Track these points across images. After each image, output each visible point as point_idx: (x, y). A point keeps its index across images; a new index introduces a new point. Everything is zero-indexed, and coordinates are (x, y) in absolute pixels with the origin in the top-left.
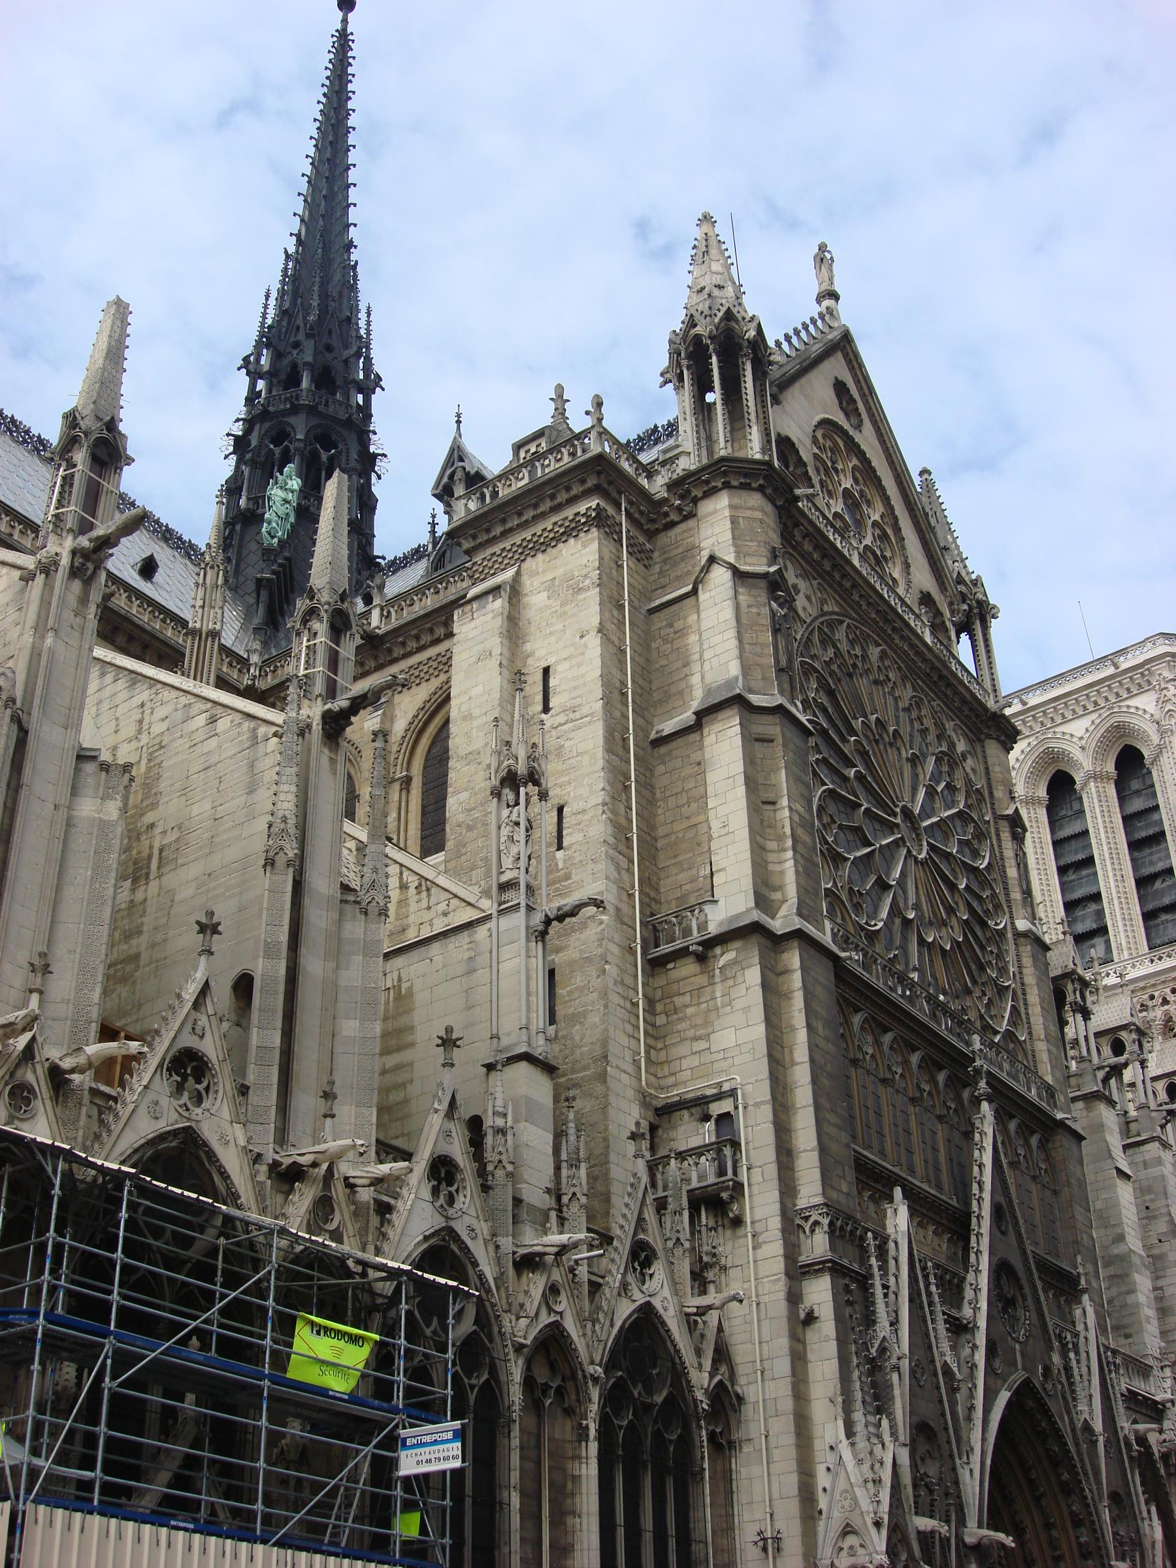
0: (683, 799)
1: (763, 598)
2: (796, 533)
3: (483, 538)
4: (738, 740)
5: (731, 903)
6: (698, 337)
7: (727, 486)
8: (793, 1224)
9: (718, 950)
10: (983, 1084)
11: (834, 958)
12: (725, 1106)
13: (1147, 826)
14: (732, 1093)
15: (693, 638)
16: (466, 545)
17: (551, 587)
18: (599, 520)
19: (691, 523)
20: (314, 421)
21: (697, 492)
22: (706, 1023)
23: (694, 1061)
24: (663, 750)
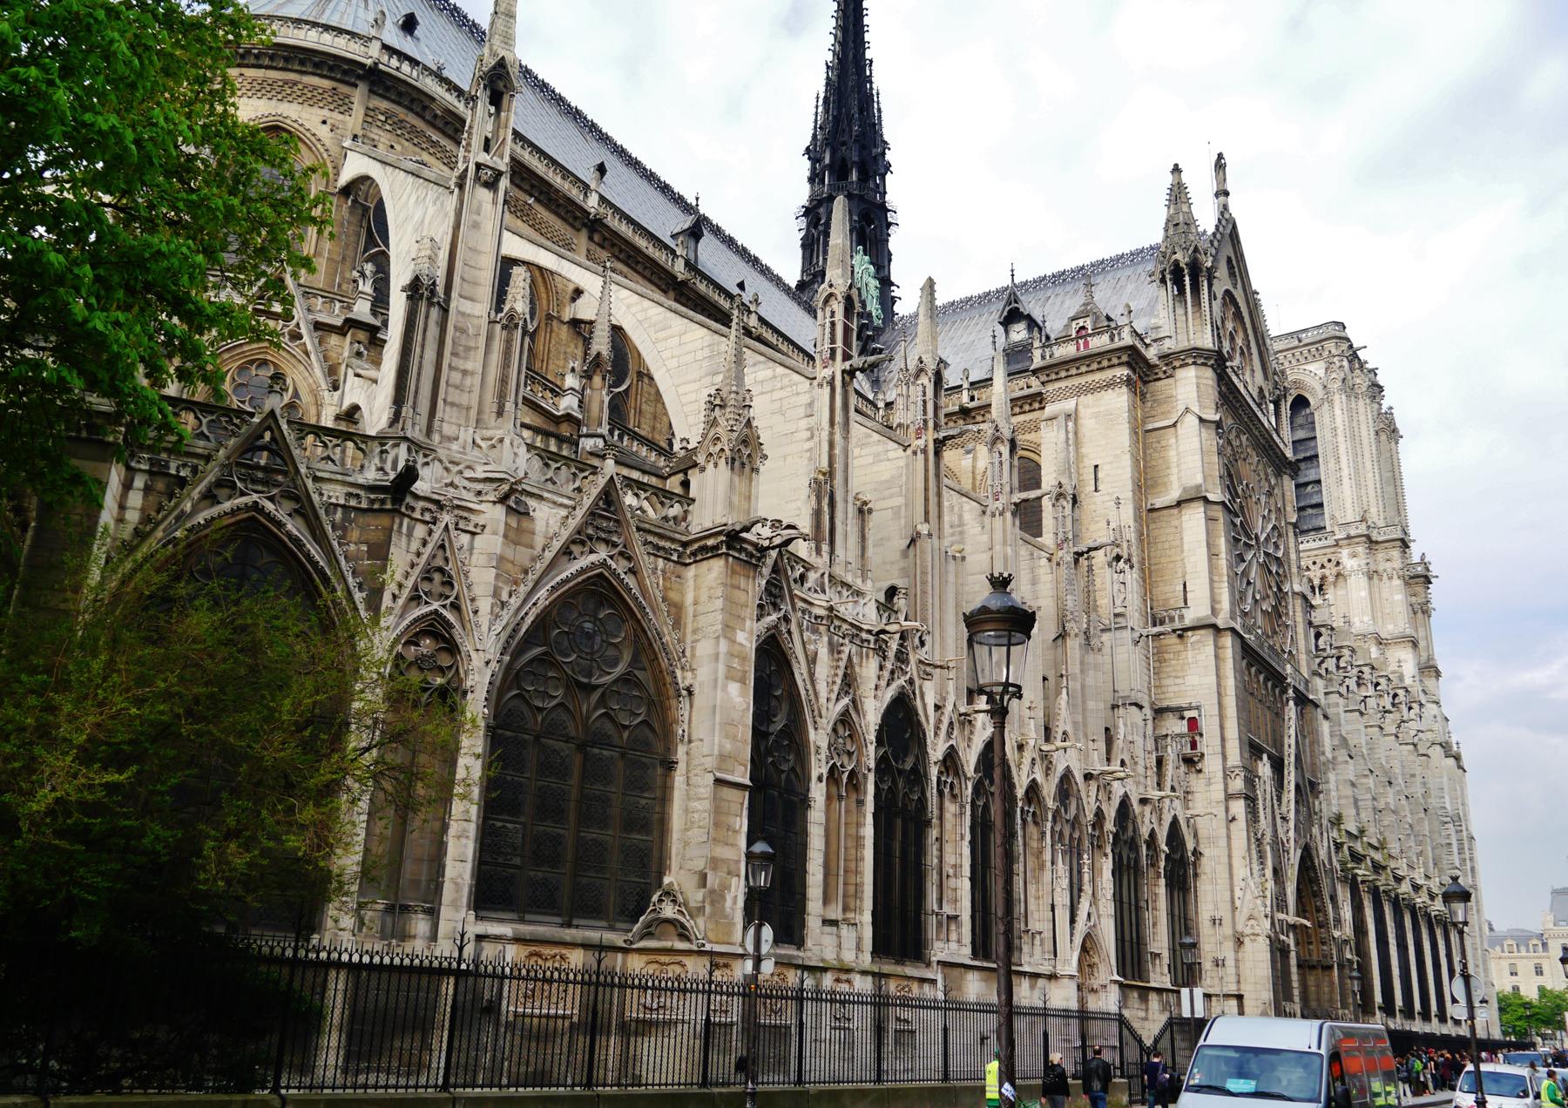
2: (1229, 396)
3: (1053, 377)
5: (1197, 610)
6: (1176, 261)
8: (1227, 775)
10: (1290, 691)
11: (1242, 637)
12: (1193, 714)
14: (1198, 708)
15: (1172, 453)
16: (1044, 378)
17: (1096, 416)
18: (1129, 382)
19: (1170, 380)
20: (863, 206)
21: (1177, 364)
24: (1155, 515)
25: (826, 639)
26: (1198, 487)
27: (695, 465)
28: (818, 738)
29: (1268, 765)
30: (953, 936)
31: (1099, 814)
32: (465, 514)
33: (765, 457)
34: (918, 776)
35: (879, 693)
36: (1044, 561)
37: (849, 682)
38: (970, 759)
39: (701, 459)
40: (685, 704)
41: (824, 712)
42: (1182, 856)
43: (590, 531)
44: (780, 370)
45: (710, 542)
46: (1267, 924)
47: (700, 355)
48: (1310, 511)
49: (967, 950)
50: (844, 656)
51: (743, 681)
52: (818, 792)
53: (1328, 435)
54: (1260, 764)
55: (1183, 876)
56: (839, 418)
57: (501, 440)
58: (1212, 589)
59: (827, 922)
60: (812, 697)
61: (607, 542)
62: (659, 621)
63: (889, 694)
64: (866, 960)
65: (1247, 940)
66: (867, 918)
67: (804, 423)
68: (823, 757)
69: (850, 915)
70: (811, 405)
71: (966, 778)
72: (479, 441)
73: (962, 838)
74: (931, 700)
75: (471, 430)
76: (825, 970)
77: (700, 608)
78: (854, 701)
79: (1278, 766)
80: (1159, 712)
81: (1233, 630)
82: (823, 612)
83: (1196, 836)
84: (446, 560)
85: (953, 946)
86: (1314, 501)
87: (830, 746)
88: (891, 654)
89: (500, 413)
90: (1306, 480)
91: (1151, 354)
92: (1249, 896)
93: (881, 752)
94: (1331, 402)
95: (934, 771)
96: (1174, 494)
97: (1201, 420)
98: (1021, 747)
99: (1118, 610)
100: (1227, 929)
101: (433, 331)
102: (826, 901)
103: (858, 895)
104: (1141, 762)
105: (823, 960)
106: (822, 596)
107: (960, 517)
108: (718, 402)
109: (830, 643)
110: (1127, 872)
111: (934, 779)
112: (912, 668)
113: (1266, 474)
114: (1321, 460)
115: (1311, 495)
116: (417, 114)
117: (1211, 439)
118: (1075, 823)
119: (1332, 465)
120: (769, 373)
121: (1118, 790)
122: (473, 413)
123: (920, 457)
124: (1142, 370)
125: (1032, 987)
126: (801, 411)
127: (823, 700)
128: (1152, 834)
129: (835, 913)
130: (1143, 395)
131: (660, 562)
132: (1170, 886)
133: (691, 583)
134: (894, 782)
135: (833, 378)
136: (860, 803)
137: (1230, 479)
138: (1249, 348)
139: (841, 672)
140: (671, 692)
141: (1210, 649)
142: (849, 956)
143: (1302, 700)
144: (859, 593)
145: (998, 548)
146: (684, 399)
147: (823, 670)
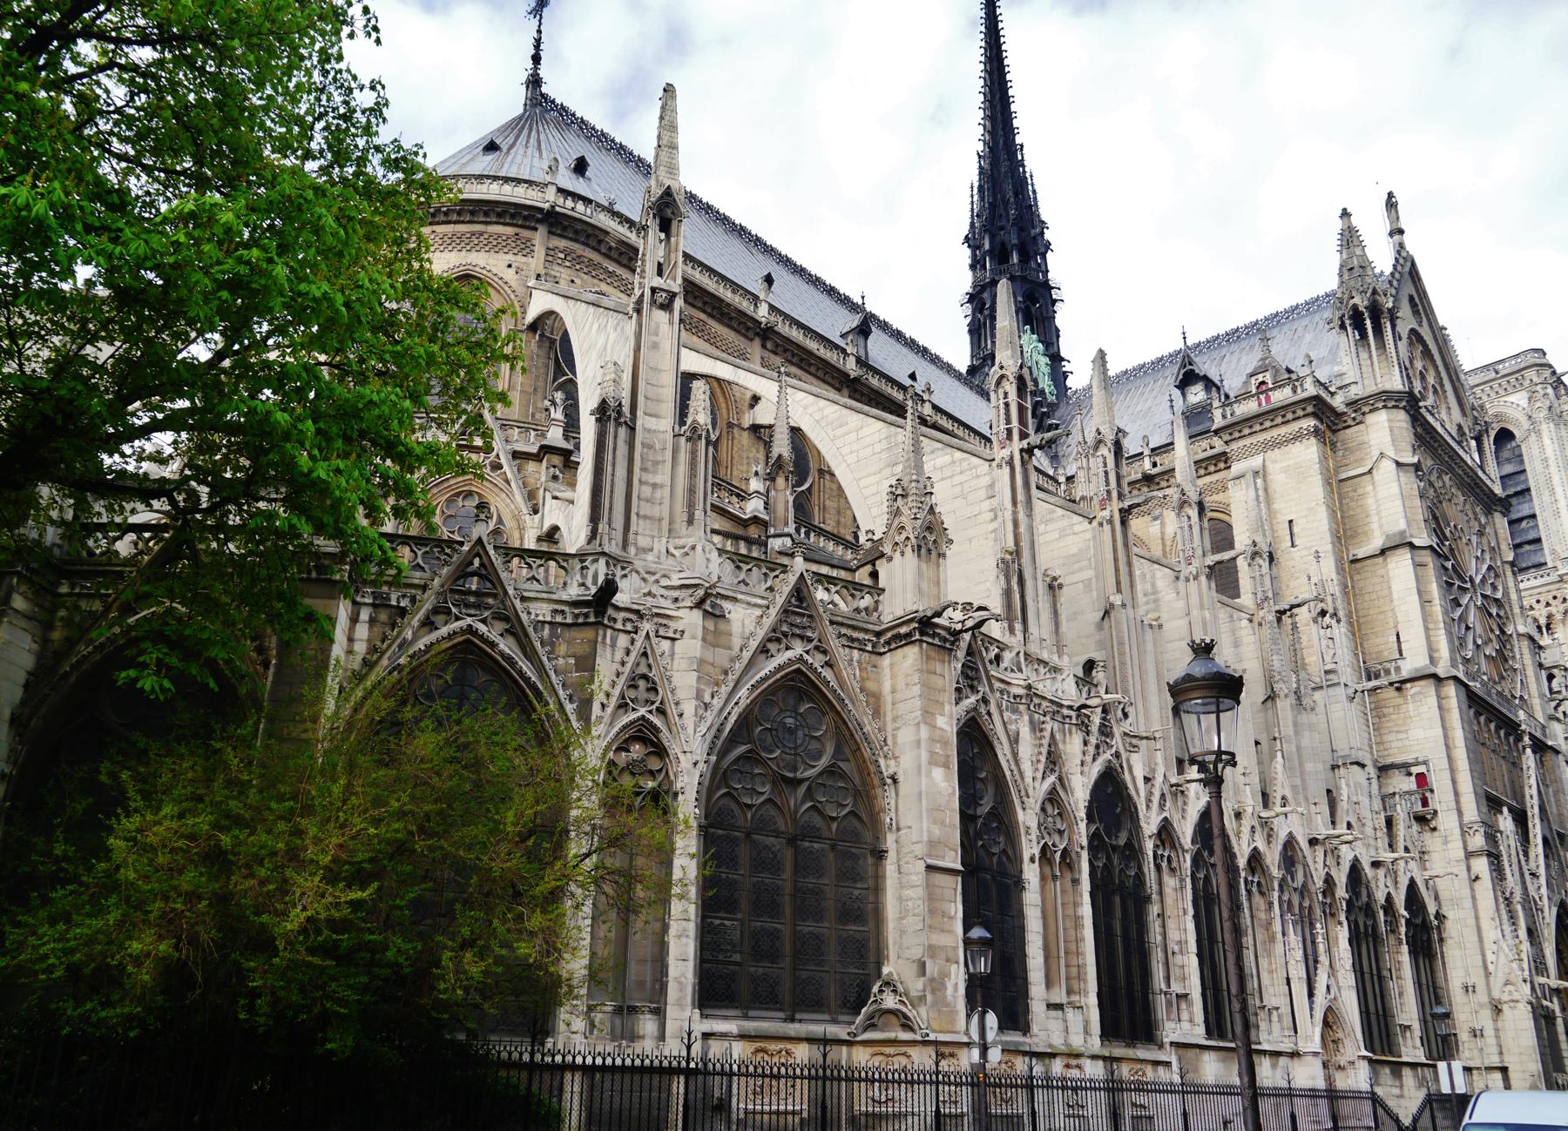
0: (1374, 596)
1: (1413, 478)
2: (1426, 436)
3: (1237, 435)
4: (1411, 568)
5: (1414, 661)
7: (1385, 407)
9: (1408, 685)
13: (1517, 484)
14: (1425, 763)
15: (1370, 501)
17: (1286, 470)
18: (1316, 432)
21: (1366, 409)
22: (1405, 724)
23: (1400, 744)
24: (1358, 565)
25: (1026, 718)
26: (1402, 533)
27: (883, 555)
28: (1027, 817)
29: (1510, 819)
30: (1185, 1016)
31: (1329, 881)
32: (664, 621)
33: (951, 542)
34: (1132, 851)
35: (1086, 769)
36: (1245, 623)
37: (1053, 760)
38: (1186, 831)
39: (887, 549)
40: (891, 791)
41: (1031, 791)
42: (1424, 921)
43: (785, 628)
44: (958, 454)
45: (903, 630)
46: (1527, 989)
47: (878, 448)
48: (1527, 547)
49: (1201, 1030)
50: (1047, 734)
51: (946, 766)
52: (1031, 873)
53: (1538, 466)
54: (1500, 818)
55: (1425, 939)
56: (1021, 497)
57: (693, 548)
58: (1428, 638)
59: (1052, 1006)
60: (1017, 777)
61: (802, 637)
62: (858, 711)
63: (1096, 769)
64: (1095, 1044)
65: (1505, 1007)
66: (1093, 1000)
67: (986, 505)
68: (1033, 837)
69: (1075, 998)
70: (992, 486)
71: (1184, 851)
72: (672, 550)
73: (1185, 913)
74: (1139, 774)
75: (664, 540)
76: (1053, 1056)
77: (898, 696)
78: (1060, 779)
79: (1521, 819)
80: (1384, 770)
81: (1455, 678)
82: (1021, 691)
83: (1437, 898)
84: (649, 666)
85: (1185, 1025)
86: (1531, 537)
87: (1040, 825)
88: (1094, 728)
89: (690, 522)
90: (1520, 515)
91: (1338, 402)
92: (1502, 960)
93: (1093, 828)
94: (1538, 433)
95: (1149, 846)
96: (1377, 543)
97: (1398, 464)
98: (1238, 815)
99: (1328, 667)
100: (1481, 997)
101: (622, 449)
102: (1049, 984)
103: (1081, 977)
104: (1369, 824)
105: (1050, 1046)
106: (1019, 675)
107: (1153, 585)
108: (899, 491)
109: (1031, 722)
110: (1365, 940)
111: (1150, 853)
112: (1117, 742)
113: (1475, 513)
114: (1533, 493)
115: (1526, 531)
116: (593, 248)
117: (1411, 483)
118: (1303, 891)
119: (1546, 497)
120: (948, 458)
121: (1347, 854)
122: (665, 524)
123: (1107, 528)
124: (1329, 419)
125: (1274, 1066)
126: (983, 494)
127: (1028, 780)
128: (1389, 898)
129: (1059, 996)
130: (1333, 445)
131: (856, 653)
132: (1413, 952)
133: (887, 672)
134: (1109, 858)
135: (1012, 458)
136: (1076, 882)
137: (1436, 521)
138: (1442, 385)
139: (1044, 750)
140: (876, 781)
141: (1432, 701)
142: (1077, 1041)
143: (1540, 747)
144: (1056, 670)
145: (1195, 613)
146: (867, 492)
147: (1026, 750)
